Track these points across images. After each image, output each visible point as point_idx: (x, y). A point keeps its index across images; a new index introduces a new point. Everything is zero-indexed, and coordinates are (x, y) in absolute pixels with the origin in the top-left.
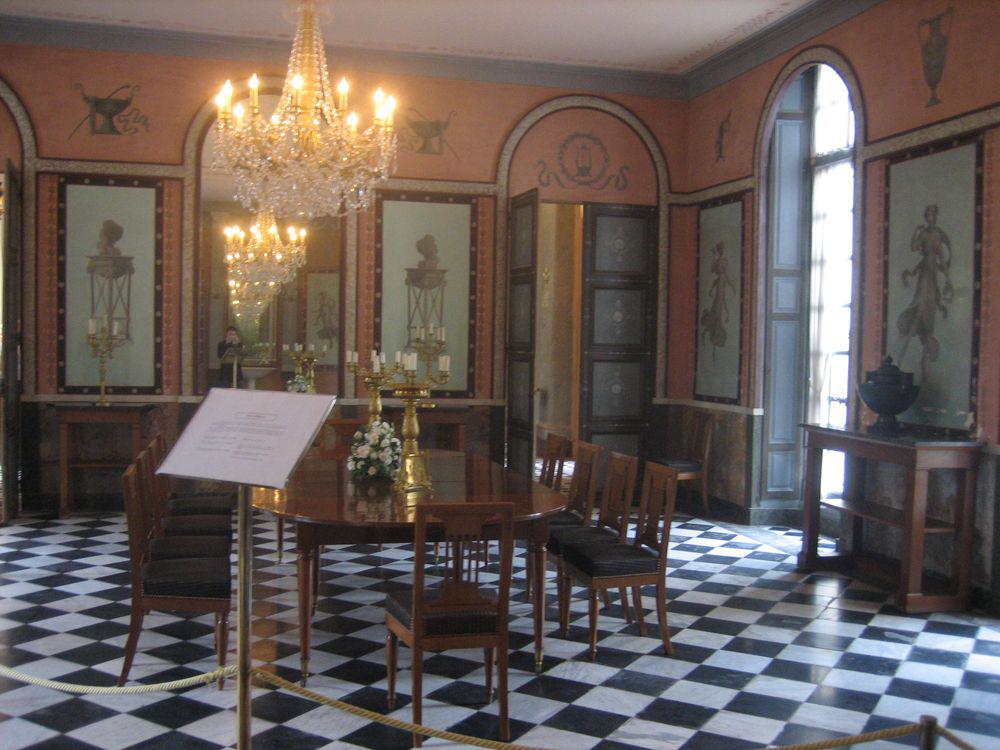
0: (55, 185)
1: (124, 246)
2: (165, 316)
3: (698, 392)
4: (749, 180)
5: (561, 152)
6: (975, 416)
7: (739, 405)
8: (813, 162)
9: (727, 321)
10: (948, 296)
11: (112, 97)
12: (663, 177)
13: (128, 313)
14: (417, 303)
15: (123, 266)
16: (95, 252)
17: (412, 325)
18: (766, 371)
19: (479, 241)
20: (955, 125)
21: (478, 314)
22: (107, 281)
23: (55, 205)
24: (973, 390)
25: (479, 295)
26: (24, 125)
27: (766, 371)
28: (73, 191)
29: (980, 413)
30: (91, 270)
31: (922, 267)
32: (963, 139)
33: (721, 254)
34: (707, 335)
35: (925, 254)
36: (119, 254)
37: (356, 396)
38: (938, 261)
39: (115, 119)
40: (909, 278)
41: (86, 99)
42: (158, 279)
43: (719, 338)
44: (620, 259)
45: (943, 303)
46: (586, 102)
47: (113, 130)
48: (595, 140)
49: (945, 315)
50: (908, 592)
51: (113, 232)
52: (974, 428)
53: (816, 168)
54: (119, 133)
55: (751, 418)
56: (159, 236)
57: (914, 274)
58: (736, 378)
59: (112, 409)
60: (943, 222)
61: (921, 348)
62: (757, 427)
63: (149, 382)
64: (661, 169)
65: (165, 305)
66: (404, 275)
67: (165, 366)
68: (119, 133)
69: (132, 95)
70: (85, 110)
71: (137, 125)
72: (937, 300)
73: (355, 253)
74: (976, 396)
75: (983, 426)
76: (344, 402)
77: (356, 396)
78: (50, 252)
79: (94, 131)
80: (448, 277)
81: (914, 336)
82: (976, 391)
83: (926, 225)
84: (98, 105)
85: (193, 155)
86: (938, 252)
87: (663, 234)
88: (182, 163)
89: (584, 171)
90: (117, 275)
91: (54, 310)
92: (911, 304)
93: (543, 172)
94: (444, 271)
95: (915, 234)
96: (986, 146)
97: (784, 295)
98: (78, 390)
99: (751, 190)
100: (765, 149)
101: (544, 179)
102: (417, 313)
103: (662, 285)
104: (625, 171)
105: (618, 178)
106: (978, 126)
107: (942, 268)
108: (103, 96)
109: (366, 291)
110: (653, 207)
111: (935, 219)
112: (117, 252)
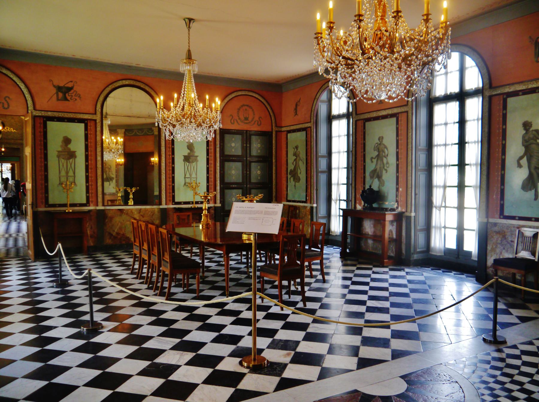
0: (42, 121)
1: (72, 147)
2: (90, 175)
3: (289, 199)
4: (309, 123)
5: (238, 112)
6: (398, 204)
7: (307, 203)
8: (331, 117)
9: (300, 173)
10: (388, 166)
11: (66, 86)
12: (273, 121)
13: (74, 173)
14: (188, 168)
15: (72, 155)
16: (60, 149)
17: (186, 177)
18: (317, 190)
19: (210, 145)
21: (210, 172)
22: (65, 161)
23: (42, 130)
24: (397, 196)
25: (210, 165)
26: (28, 96)
27: (317, 190)
28: (49, 123)
29: (399, 203)
30: (58, 157)
31: (378, 156)
32: (392, 116)
33: (297, 149)
34: (292, 179)
35: (379, 152)
36: (70, 150)
37: (166, 204)
38: (384, 155)
39: (67, 95)
40: (373, 160)
41: (54, 86)
42: (87, 160)
43: (297, 179)
44: (259, 151)
45: (385, 168)
46: (247, 93)
47: (66, 99)
48: (250, 107)
49: (386, 172)
50: (384, 259)
51: (67, 141)
52: (397, 208)
53: (332, 120)
54: (69, 101)
55: (312, 208)
56: (87, 143)
57: (375, 158)
58: (305, 194)
59: (74, 213)
60: (385, 142)
61: (378, 183)
62: (314, 210)
63: (84, 202)
64: (273, 118)
65: (90, 170)
66: (183, 158)
67: (90, 195)
68: (69, 101)
69: (74, 85)
70: (54, 91)
71: (76, 98)
72: (384, 167)
73: (164, 150)
74: (398, 197)
75: (401, 207)
76: (161, 207)
77: (166, 204)
78: (41, 149)
79: (58, 99)
80: (198, 158)
81: (375, 178)
83: (379, 143)
84: (59, 89)
85: (100, 110)
86: (383, 152)
87: (274, 142)
88: (95, 114)
89: (246, 119)
90: (69, 159)
91: (43, 173)
93: (232, 119)
94: (197, 156)
95: (375, 145)
96: (400, 119)
97: (323, 164)
98: (54, 206)
99: (310, 127)
100: (315, 115)
101: (232, 121)
102: (188, 172)
103: (274, 161)
104: (260, 119)
105: (258, 121)
106: (397, 112)
107: (385, 157)
108: (61, 85)
109: (169, 164)
110: (269, 132)
111: (382, 141)
112: (69, 149)
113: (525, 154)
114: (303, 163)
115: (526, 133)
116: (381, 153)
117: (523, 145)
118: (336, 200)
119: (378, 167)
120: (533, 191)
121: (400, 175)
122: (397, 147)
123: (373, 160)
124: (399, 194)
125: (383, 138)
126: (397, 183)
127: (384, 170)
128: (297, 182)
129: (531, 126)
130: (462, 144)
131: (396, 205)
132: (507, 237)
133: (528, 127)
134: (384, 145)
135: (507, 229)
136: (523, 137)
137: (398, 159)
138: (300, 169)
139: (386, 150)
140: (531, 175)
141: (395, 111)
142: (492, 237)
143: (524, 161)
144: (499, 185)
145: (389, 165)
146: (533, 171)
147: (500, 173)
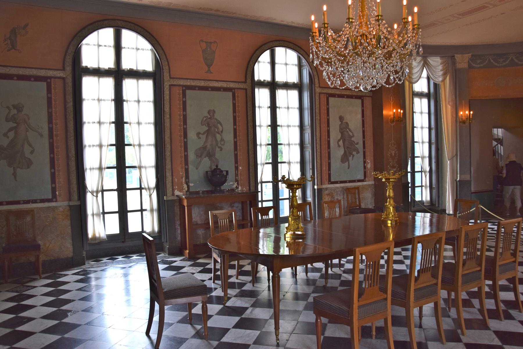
6: (238, 184)
10: (222, 143)
20: (223, 84)
29: (239, 182)
31: (208, 132)
32: (226, 90)
40: (200, 136)
45: (219, 145)
49: (221, 150)
52: (237, 188)
57: (203, 134)
72: (217, 145)
75: (241, 186)
81: (205, 157)
82: (238, 175)
86: (216, 127)
92: (202, 146)
106: (233, 87)
107: (219, 134)
111: (214, 115)
113: (342, 138)
114: (41, 135)
115: (341, 124)
116: (213, 128)
117: (340, 132)
118: (97, 192)
119: (208, 145)
120: (347, 163)
121: (238, 153)
122: (235, 123)
123: (200, 136)
124: (239, 173)
125: (214, 112)
126: (236, 162)
127: (217, 147)
128: (21, 168)
129: (344, 120)
130: (274, 126)
131: (236, 185)
132: (334, 196)
133: (342, 120)
134: (216, 119)
135: (334, 191)
136: (340, 126)
137: (235, 136)
138: (30, 145)
139: (219, 126)
140: (345, 151)
141: (232, 85)
142: (325, 199)
143: (341, 143)
144: (327, 160)
145: (224, 143)
146: (346, 150)
147: (327, 151)
